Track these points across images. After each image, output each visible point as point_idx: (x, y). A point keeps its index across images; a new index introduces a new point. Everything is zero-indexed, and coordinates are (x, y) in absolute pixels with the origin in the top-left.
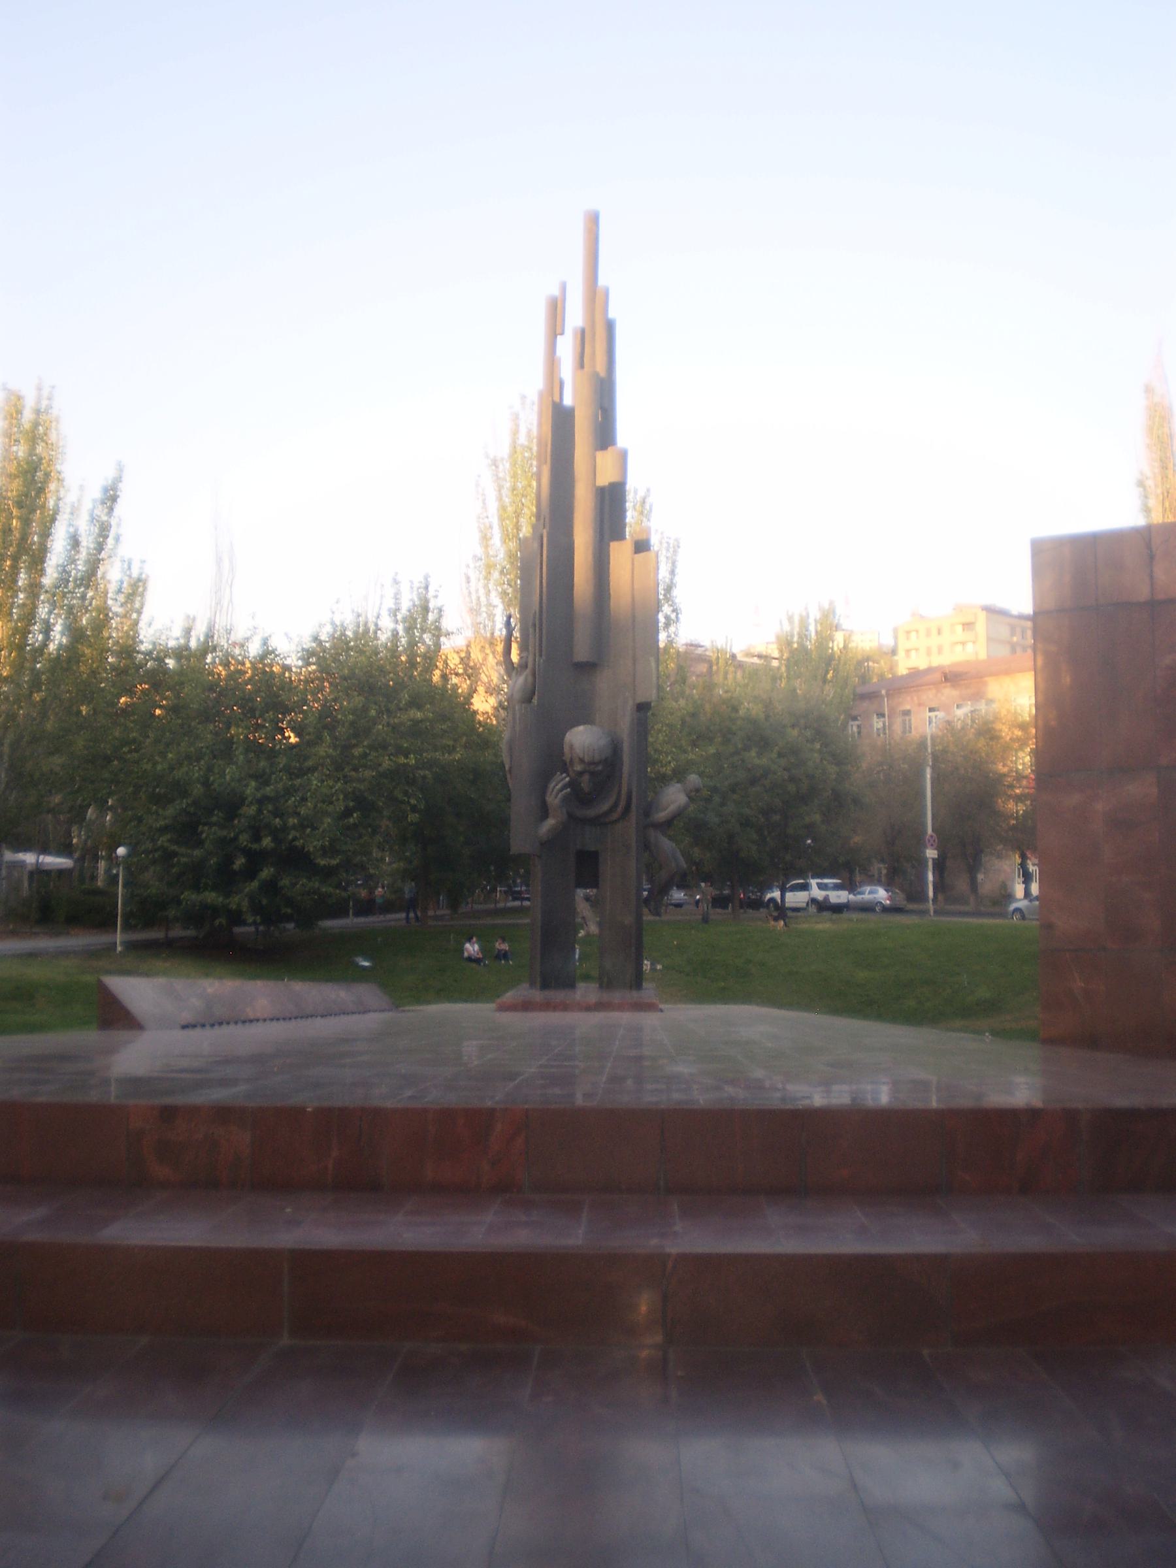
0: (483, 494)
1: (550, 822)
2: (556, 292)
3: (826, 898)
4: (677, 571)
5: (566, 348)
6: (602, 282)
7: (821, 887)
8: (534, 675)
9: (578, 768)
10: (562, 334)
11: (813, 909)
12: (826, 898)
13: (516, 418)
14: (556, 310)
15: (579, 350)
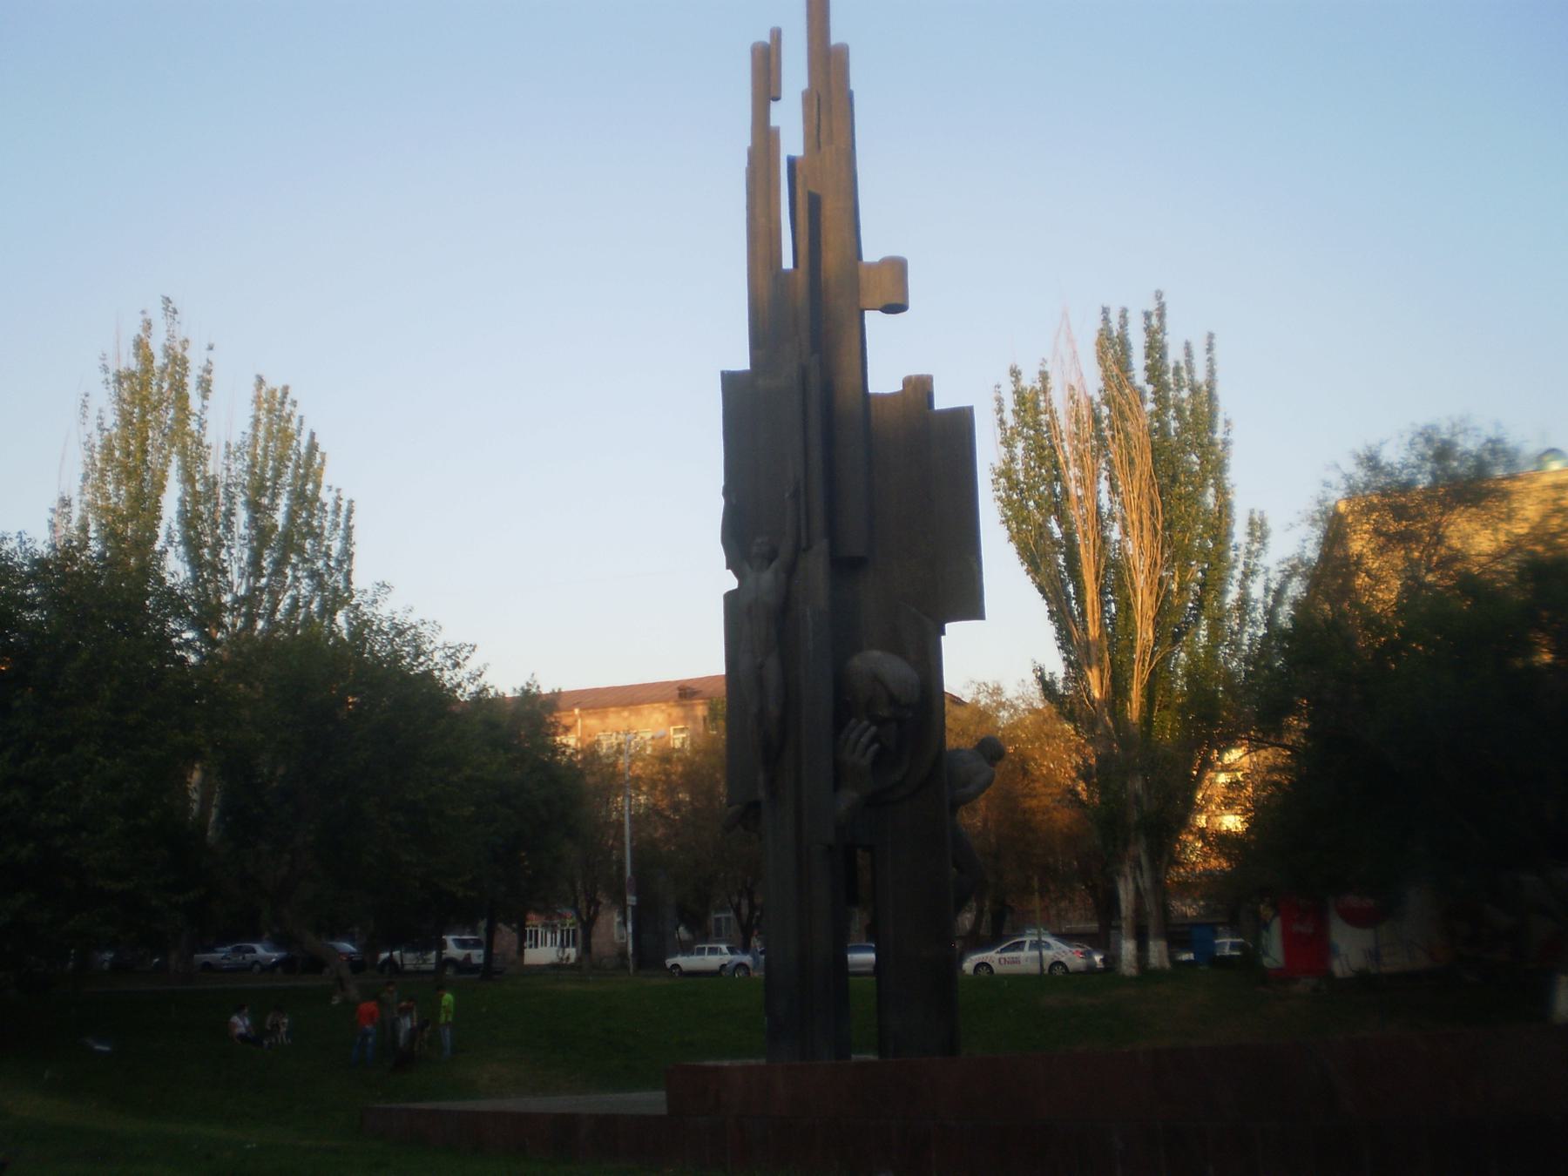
0: (84, 416)
1: (848, 798)
2: (766, 38)
3: (468, 957)
4: (354, 538)
5: (789, 120)
6: (835, 39)
7: (462, 944)
8: (791, 570)
9: (884, 712)
10: (777, 99)
11: (449, 972)
12: (468, 957)
13: (148, 325)
14: (766, 63)
15: (815, 122)
